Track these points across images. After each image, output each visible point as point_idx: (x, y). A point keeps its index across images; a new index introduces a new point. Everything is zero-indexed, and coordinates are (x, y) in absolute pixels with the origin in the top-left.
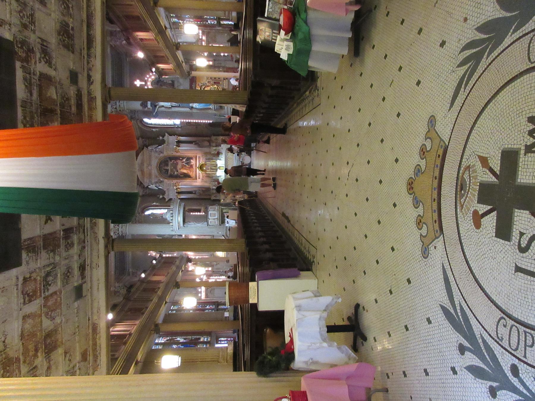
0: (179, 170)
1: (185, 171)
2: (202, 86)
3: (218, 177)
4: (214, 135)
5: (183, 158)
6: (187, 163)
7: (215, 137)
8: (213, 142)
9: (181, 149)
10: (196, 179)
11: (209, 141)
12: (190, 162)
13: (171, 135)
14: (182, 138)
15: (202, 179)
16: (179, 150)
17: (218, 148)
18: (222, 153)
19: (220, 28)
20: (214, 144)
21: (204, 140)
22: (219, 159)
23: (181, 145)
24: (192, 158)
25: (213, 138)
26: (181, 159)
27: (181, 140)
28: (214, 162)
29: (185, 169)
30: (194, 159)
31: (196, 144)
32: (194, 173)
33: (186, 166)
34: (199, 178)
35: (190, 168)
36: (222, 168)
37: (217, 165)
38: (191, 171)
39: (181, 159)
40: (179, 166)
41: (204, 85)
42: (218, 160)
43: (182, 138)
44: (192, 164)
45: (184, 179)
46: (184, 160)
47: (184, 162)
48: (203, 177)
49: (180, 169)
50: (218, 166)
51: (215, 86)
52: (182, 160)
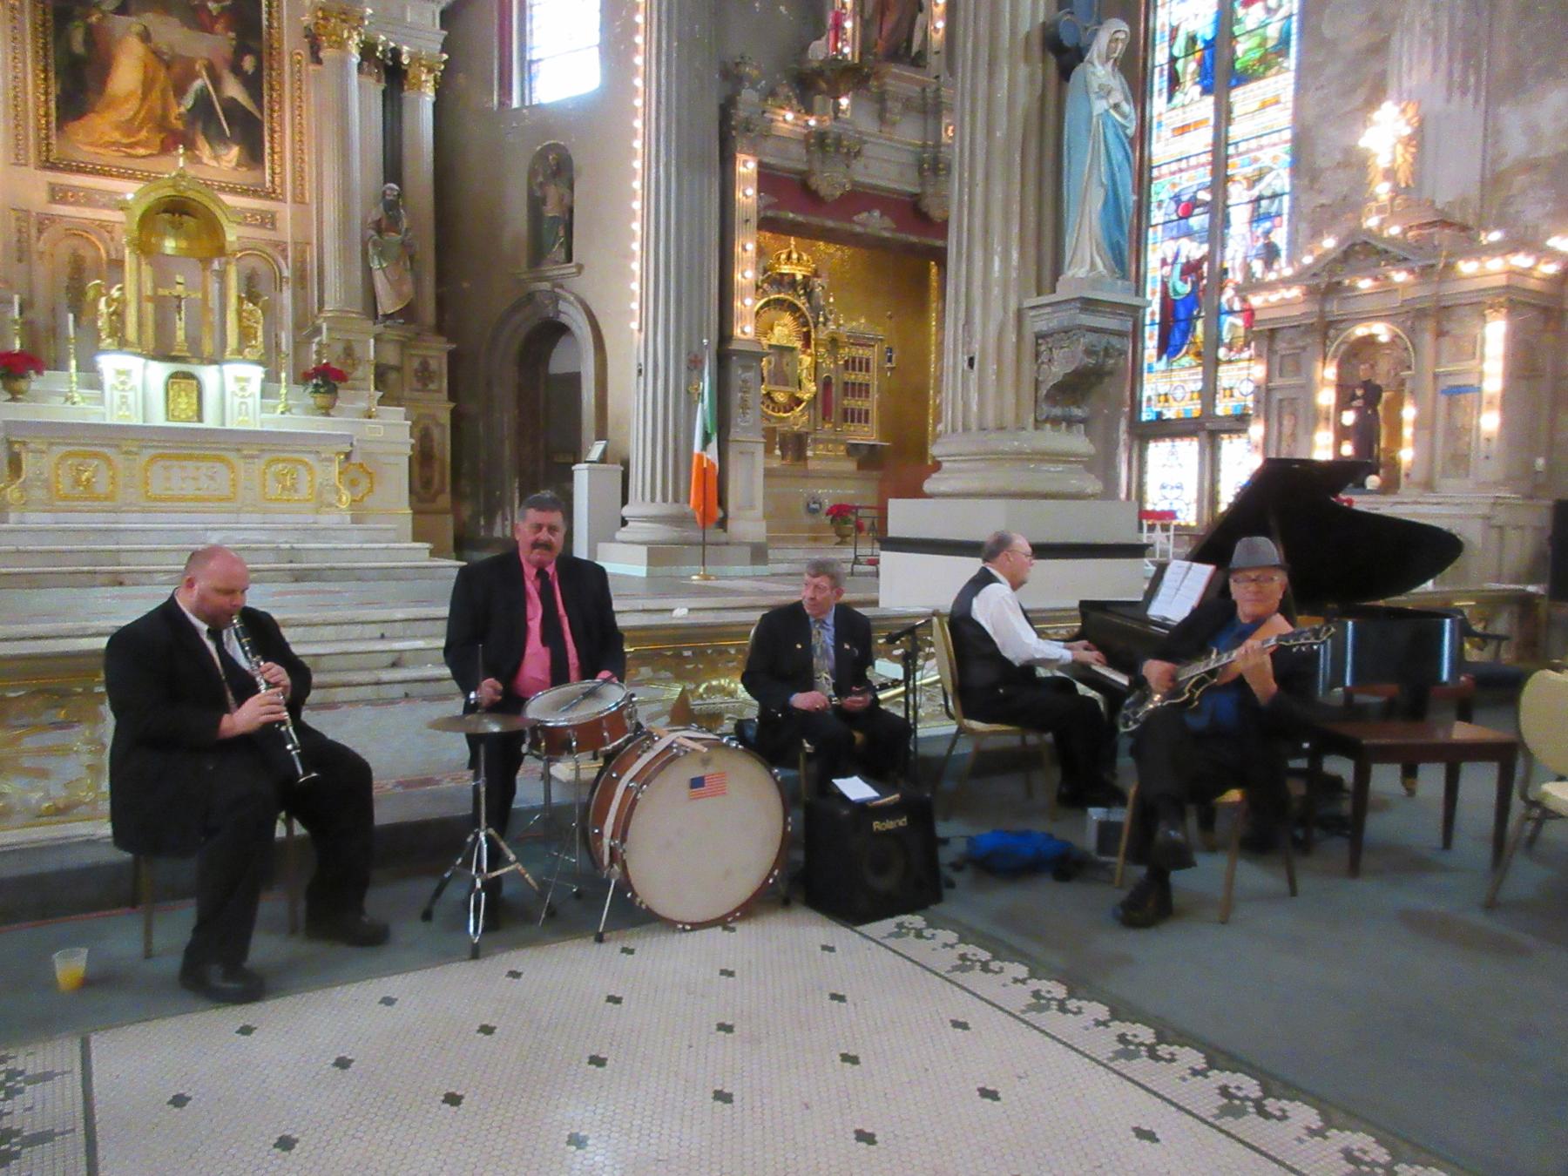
0: (133, 24)
1: (127, 74)
2: (809, 295)
3: (89, 368)
4: (454, 359)
5: (253, 84)
6: (203, 107)
7: (439, 364)
8: (403, 345)
9: (344, 63)
10: (52, 166)
11: (408, 313)
12: (217, 138)
13: (447, 18)
14: (423, 103)
15: (44, 222)
16: (342, 45)
17: (366, 373)
18: (326, 411)
20: (391, 356)
21: (418, 282)
22: (271, 378)
23: (376, 89)
24: (254, 155)
25: (437, 352)
26: (248, 63)
27: (408, 94)
28: (245, 335)
29: (148, 85)
30: (246, 176)
31: (391, 207)
32: (110, 157)
33: (180, 91)
34: (58, 194)
35: (162, 125)
36: (185, 403)
37: (216, 360)
38: (128, 127)
39: (248, 63)
40: (172, 33)
41: (816, 309)
42: (257, 373)
43: (423, 103)
44: (205, 151)
45: (43, 54)
46: (234, 89)
47: (216, 81)
48: (78, 232)
49: (145, 37)
50: (209, 375)
51: (812, 387)
52: (237, 70)
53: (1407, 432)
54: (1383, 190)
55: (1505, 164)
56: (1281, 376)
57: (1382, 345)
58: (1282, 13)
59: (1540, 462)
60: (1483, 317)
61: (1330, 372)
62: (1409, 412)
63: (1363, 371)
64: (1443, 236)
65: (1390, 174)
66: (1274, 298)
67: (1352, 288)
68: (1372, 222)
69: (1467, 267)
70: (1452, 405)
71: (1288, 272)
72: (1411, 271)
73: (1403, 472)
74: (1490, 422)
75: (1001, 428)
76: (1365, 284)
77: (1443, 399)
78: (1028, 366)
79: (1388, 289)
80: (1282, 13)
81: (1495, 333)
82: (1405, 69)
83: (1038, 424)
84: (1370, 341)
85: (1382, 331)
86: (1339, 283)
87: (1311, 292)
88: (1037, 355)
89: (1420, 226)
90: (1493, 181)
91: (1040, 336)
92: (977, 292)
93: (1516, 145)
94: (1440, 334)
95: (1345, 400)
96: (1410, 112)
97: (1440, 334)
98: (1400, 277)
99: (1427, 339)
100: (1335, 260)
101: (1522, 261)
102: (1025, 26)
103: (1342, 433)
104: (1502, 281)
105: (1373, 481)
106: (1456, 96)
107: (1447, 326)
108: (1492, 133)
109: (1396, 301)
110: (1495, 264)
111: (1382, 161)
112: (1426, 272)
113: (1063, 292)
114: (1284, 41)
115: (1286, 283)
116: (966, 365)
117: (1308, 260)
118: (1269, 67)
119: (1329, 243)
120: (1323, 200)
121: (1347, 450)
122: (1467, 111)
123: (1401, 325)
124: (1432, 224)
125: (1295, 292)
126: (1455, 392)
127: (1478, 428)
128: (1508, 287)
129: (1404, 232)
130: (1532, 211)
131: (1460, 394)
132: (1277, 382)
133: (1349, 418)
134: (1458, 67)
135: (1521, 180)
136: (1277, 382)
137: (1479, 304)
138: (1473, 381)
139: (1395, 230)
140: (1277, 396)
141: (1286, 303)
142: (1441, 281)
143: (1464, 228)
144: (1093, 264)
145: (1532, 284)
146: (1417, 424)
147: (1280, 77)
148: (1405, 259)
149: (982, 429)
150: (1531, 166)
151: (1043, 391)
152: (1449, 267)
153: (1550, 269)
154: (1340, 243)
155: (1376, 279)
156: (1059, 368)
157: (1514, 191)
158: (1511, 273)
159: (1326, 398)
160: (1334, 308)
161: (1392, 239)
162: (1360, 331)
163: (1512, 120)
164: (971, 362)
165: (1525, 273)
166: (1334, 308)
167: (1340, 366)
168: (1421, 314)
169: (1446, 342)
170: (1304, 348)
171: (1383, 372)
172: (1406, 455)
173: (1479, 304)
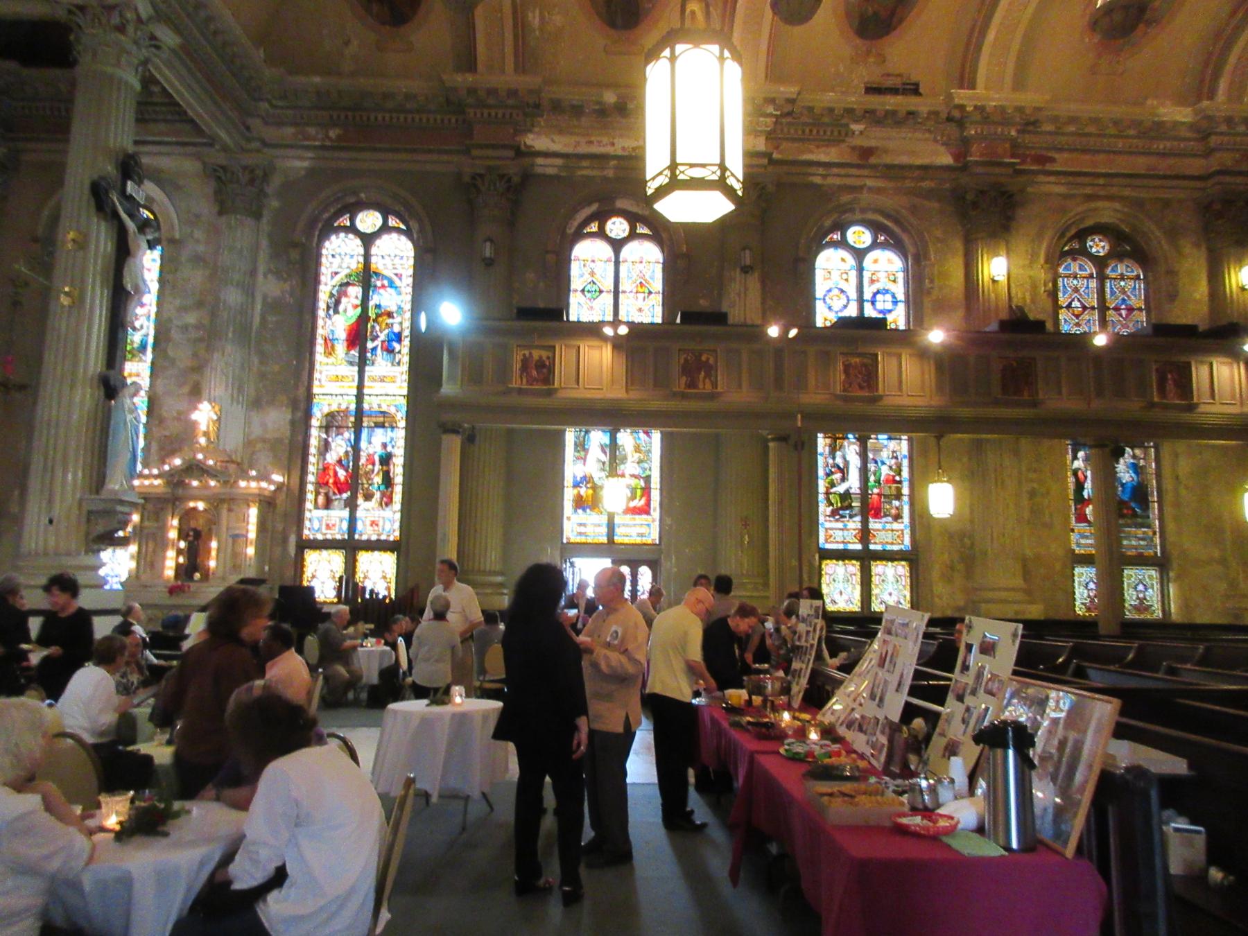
19: (292, 550)
53: (214, 553)
54: (203, 441)
55: (253, 437)
56: (148, 519)
57: (200, 512)
58: (143, 332)
59: (267, 568)
60: (249, 506)
61: (175, 522)
62: (214, 544)
63: (193, 524)
64: (232, 467)
65: (206, 434)
66: (147, 482)
67: (189, 484)
68: (200, 456)
69: (243, 484)
70: (234, 542)
71: (155, 471)
72: (218, 481)
73: (211, 571)
74: (251, 551)
75: (68, 554)
76: (195, 483)
77: (230, 540)
78: (83, 528)
79: (207, 487)
80: (143, 332)
81: (253, 513)
82: (212, 386)
83: (86, 552)
84: (195, 509)
85: (201, 506)
86: (183, 481)
87: (168, 483)
88: (88, 520)
89: (222, 462)
90: (249, 444)
91: (90, 513)
92: (58, 489)
93: (257, 431)
94: (230, 510)
95: (180, 537)
96: (217, 408)
97: (230, 510)
98: (212, 483)
99: (224, 512)
100: (182, 470)
101: (264, 485)
102: (91, 370)
103: (179, 552)
104: (257, 491)
105: (197, 576)
106: (235, 404)
107: (234, 507)
108: (248, 422)
109: (207, 493)
110: (253, 484)
111: (203, 427)
112: (226, 482)
113: (104, 494)
114: (143, 347)
115: (156, 477)
116: (47, 522)
117: (167, 468)
118: (134, 356)
119: (178, 462)
120: (167, 433)
121: (181, 560)
122: (238, 411)
123: (211, 504)
124: (227, 462)
125: (157, 482)
126: (235, 537)
127: (246, 555)
128: (259, 495)
129: (216, 464)
130: (264, 458)
131: (238, 538)
132: (146, 523)
133: (182, 544)
134: (235, 391)
135: (259, 446)
136: (146, 523)
137: (246, 500)
138: (244, 532)
139: (211, 462)
140: (146, 531)
141: (151, 486)
142: (232, 487)
143: (238, 464)
144: (122, 484)
145: (266, 493)
146: (218, 550)
147: (140, 364)
148: (216, 476)
149: (56, 554)
150: (264, 441)
151: (91, 537)
152: (236, 482)
153: (272, 488)
154: (183, 463)
155: (201, 481)
156: (100, 528)
157: (257, 449)
158: (260, 489)
159: (173, 534)
160: (180, 492)
161: (210, 466)
162: (192, 504)
163: (256, 418)
164: (51, 521)
165: (265, 489)
166: (180, 492)
167: (180, 520)
168: (222, 501)
169: (232, 514)
170: (162, 509)
171: (200, 524)
172: (212, 564)
173: (246, 500)
